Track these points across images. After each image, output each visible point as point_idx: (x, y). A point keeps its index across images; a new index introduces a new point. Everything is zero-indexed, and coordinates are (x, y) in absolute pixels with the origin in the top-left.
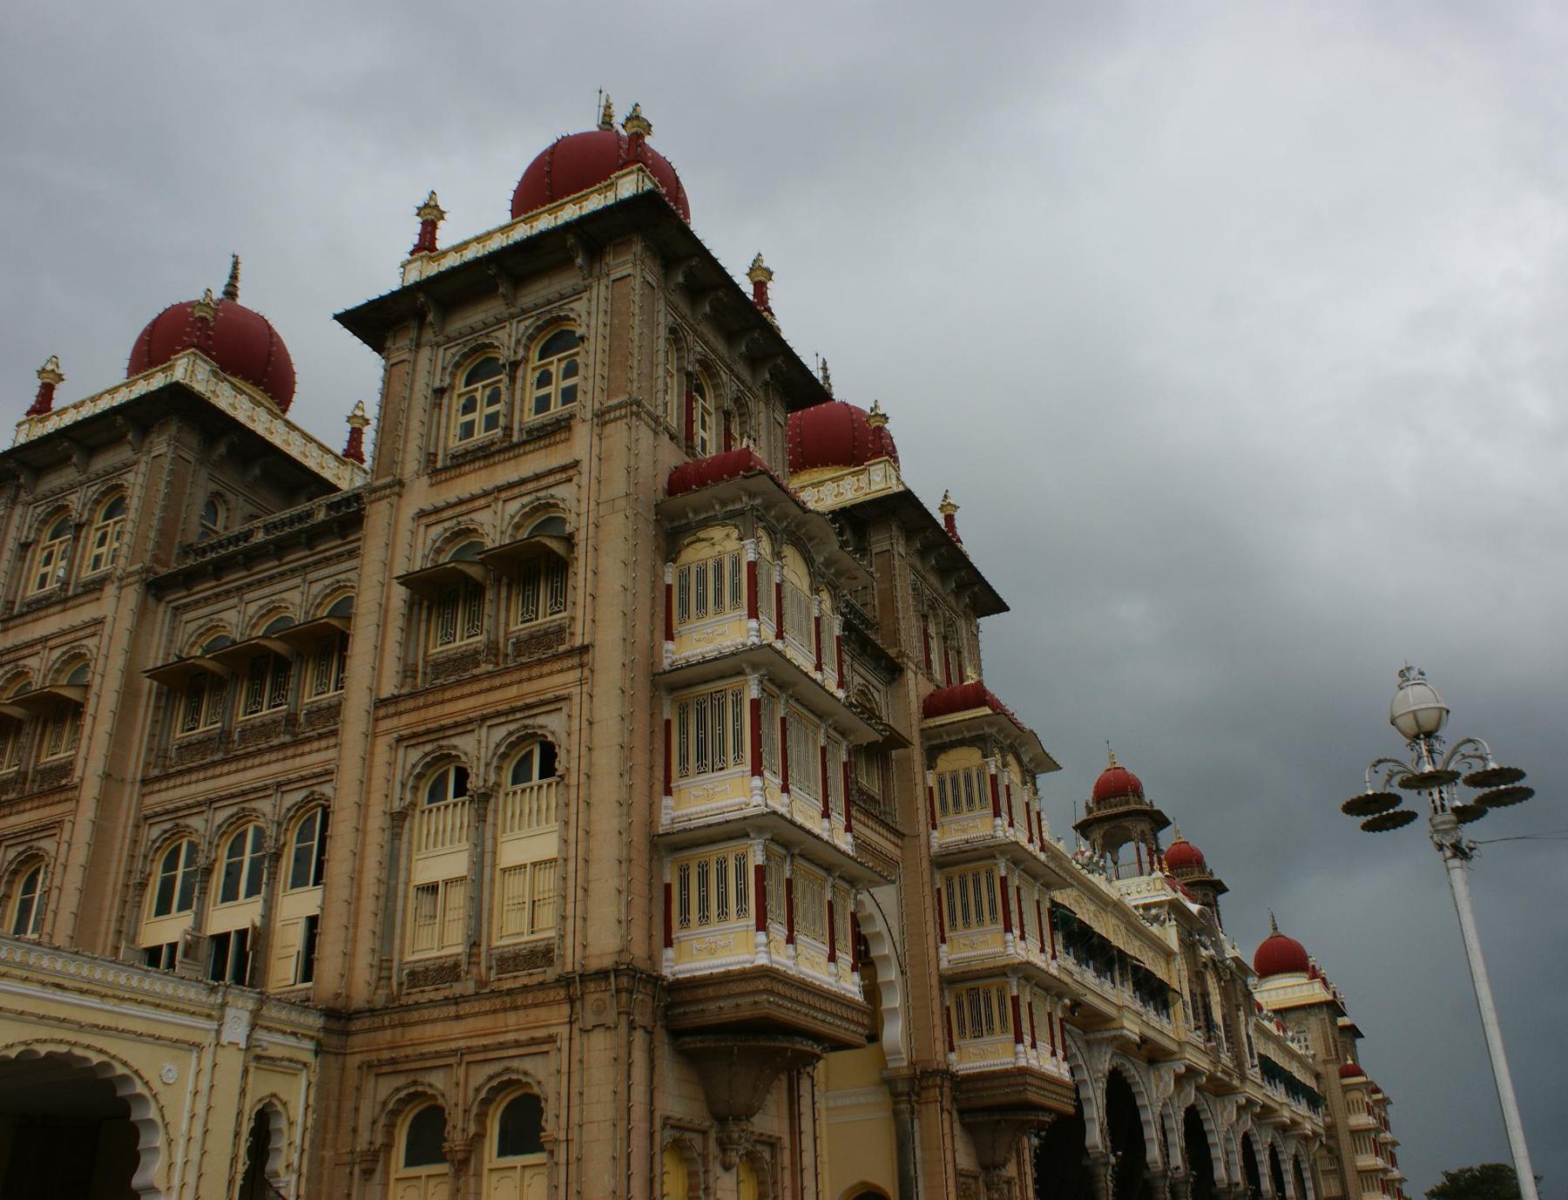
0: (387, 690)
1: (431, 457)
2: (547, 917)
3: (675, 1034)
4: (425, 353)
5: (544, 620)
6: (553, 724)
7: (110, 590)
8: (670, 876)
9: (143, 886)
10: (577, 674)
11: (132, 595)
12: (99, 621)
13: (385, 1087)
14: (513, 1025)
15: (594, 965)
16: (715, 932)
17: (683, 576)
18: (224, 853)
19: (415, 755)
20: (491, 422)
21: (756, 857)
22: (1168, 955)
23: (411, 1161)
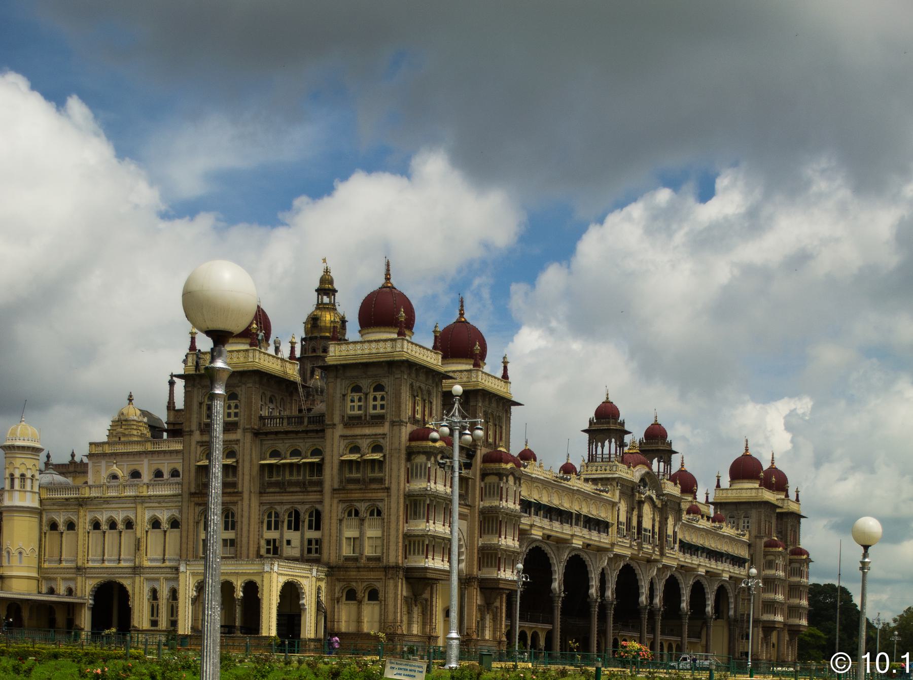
0: (336, 486)
1: (343, 417)
2: (379, 550)
3: (407, 579)
4: (339, 380)
5: (377, 474)
6: (380, 505)
7: (239, 431)
8: (407, 543)
9: (262, 522)
10: (386, 494)
11: (249, 436)
12: (238, 440)
13: (342, 584)
14: (372, 575)
15: (391, 564)
16: (416, 557)
17: (412, 466)
18: (286, 517)
19: (344, 505)
20: (360, 408)
21: (427, 542)
22: (614, 504)
23: (347, 599)
